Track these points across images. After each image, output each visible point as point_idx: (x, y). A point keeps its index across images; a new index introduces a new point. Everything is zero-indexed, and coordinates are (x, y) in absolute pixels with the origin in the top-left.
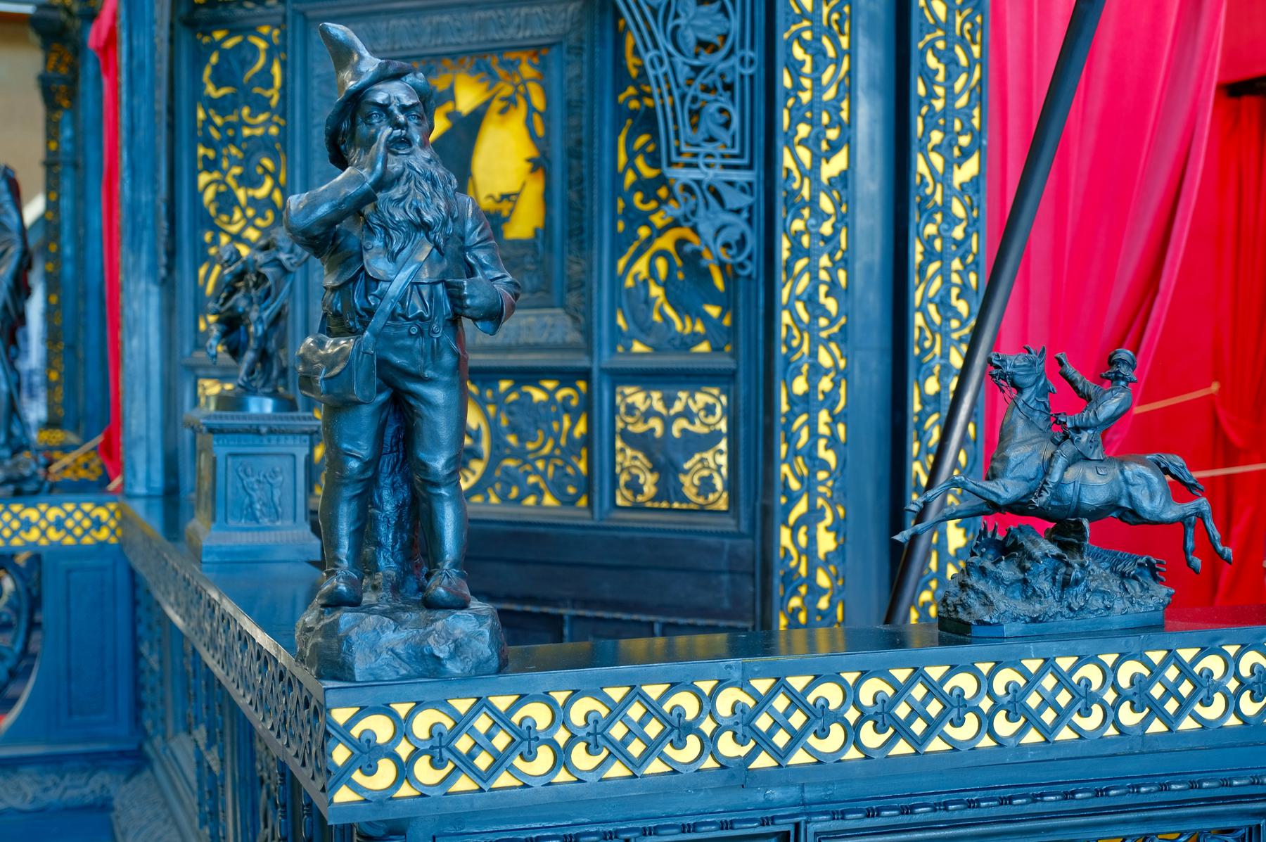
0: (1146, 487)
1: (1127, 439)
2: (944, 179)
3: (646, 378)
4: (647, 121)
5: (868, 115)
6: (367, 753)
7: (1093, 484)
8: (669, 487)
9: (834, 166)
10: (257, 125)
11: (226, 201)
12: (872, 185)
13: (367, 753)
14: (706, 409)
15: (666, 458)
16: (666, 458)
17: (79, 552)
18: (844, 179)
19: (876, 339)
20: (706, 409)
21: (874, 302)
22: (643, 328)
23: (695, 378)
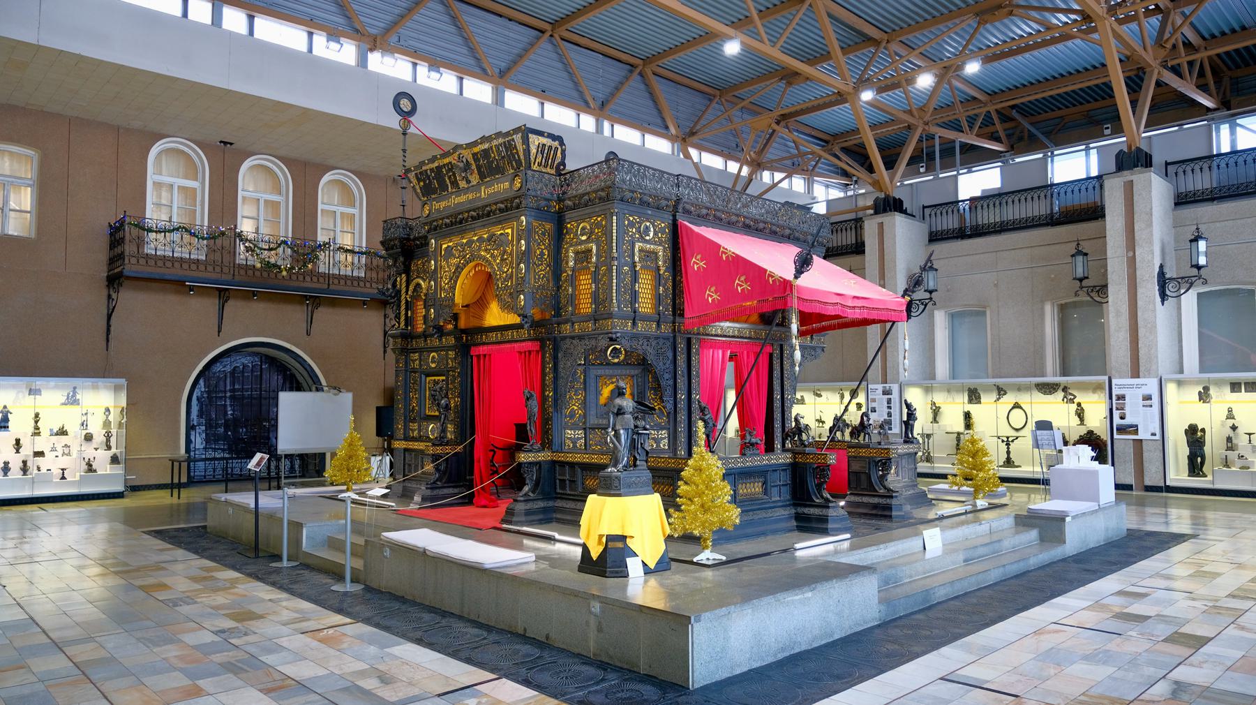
7: (754, 440)
8: (658, 445)
11: (571, 398)
14: (664, 434)
15: (657, 441)
16: (657, 441)
23: (662, 429)
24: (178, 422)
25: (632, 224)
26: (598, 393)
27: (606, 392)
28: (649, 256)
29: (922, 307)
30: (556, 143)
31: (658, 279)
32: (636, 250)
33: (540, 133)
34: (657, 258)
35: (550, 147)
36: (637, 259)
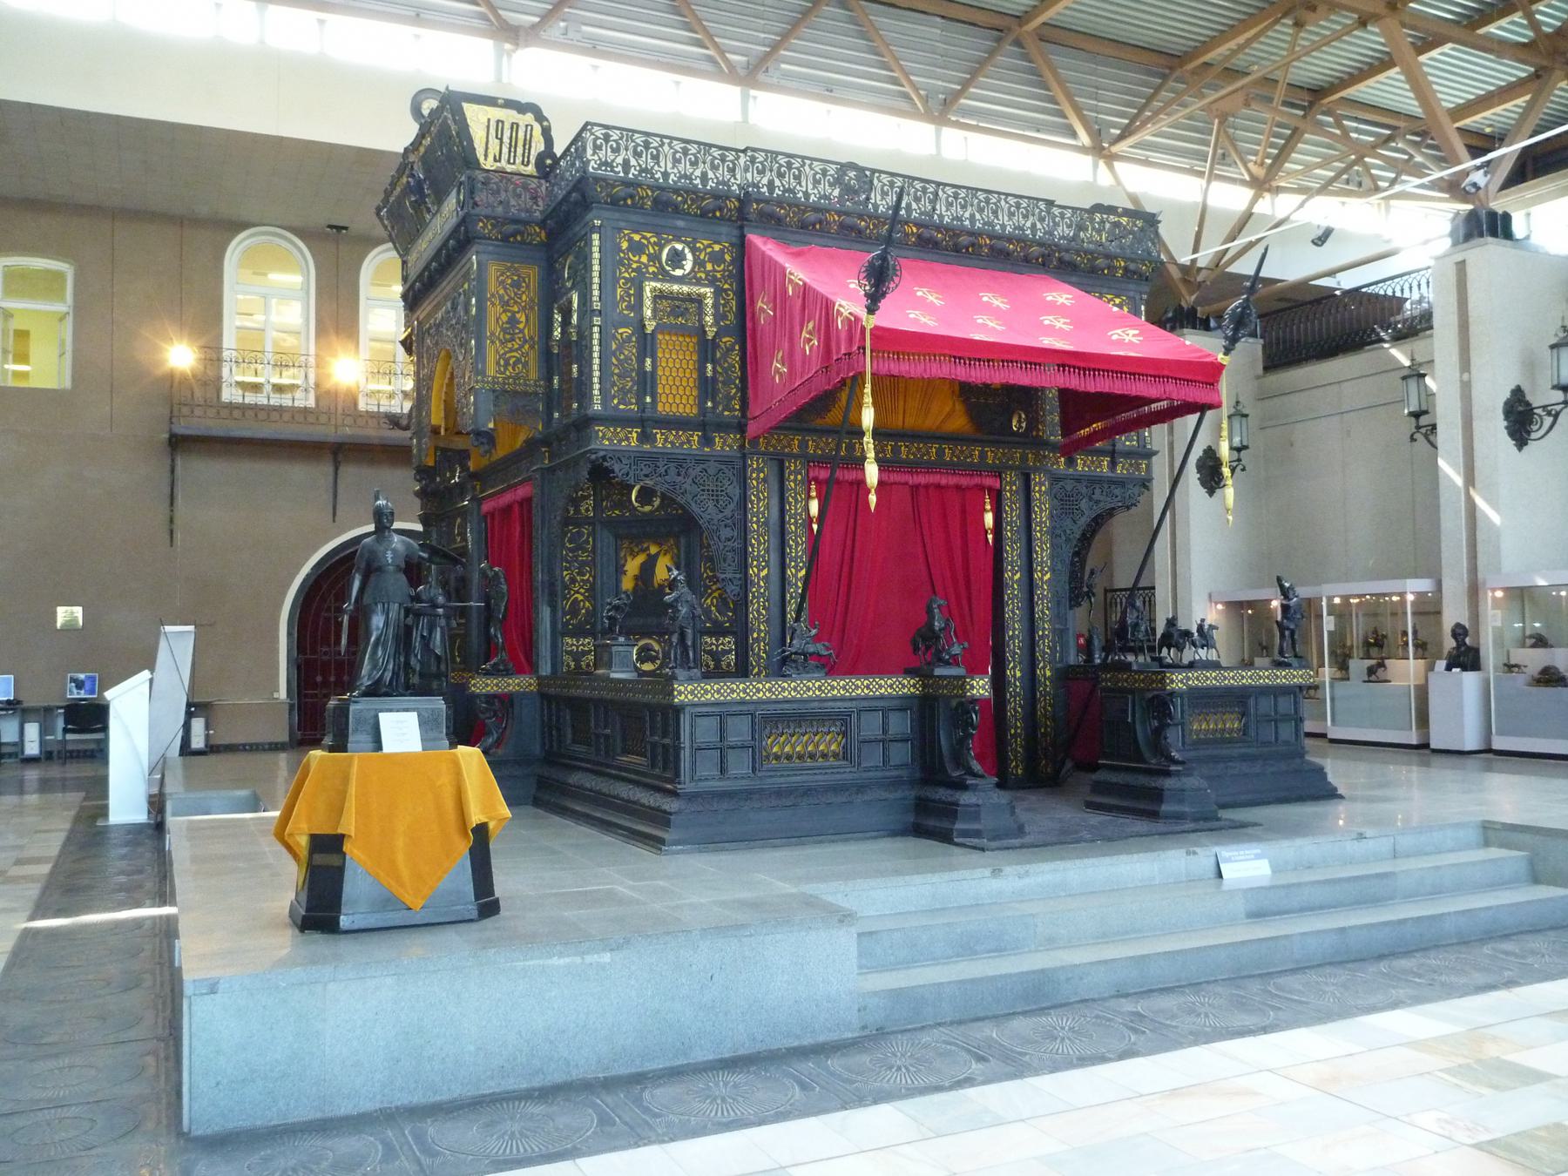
0: (820, 648)
1: (817, 639)
2: (795, 576)
3: (710, 633)
4: (711, 559)
5: (774, 558)
6: (680, 693)
7: (811, 649)
9: (763, 574)
10: (583, 557)
11: (573, 581)
12: (775, 578)
13: (680, 693)
14: (728, 642)
17: (524, 693)
18: (766, 577)
19: (776, 622)
20: (728, 642)
21: (776, 611)
22: (709, 619)
24: (276, 651)
25: (637, 248)
26: (620, 571)
27: (633, 566)
28: (679, 307)
29: (1548, 421)
30: (529, 118)
31: (706, 350)
32: (647, 293)
33: (490, 101)
34: (701, 312)
35: (515, 126)
36: (648, 313)
